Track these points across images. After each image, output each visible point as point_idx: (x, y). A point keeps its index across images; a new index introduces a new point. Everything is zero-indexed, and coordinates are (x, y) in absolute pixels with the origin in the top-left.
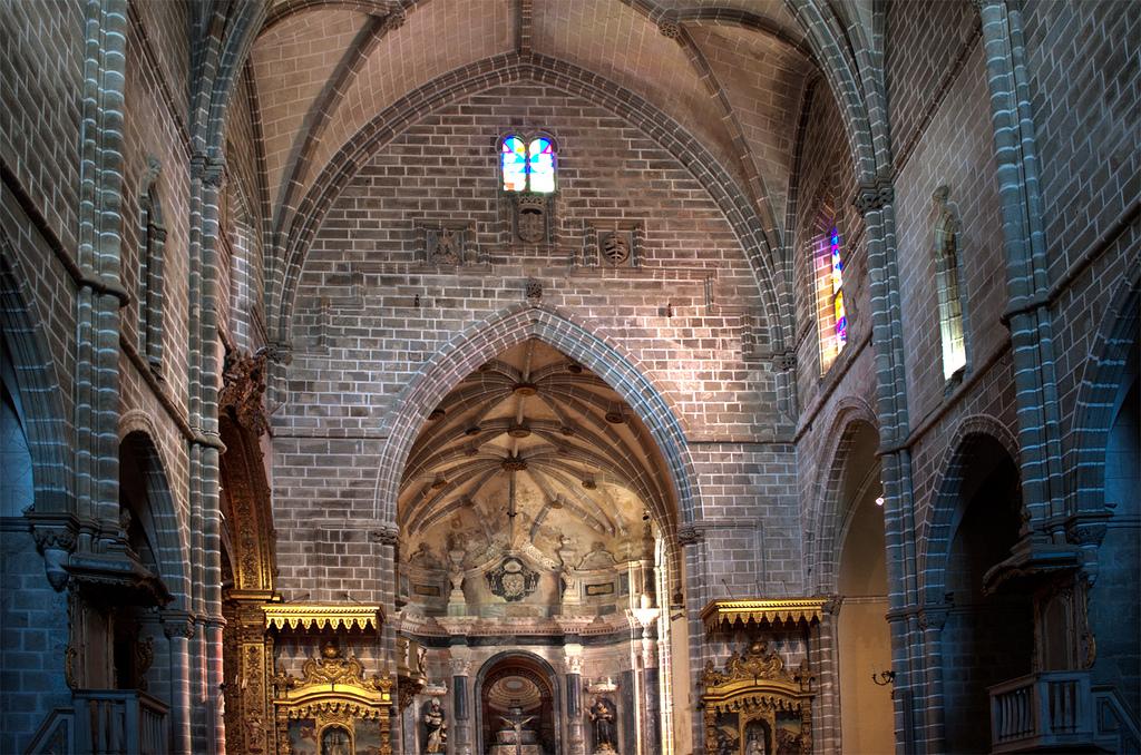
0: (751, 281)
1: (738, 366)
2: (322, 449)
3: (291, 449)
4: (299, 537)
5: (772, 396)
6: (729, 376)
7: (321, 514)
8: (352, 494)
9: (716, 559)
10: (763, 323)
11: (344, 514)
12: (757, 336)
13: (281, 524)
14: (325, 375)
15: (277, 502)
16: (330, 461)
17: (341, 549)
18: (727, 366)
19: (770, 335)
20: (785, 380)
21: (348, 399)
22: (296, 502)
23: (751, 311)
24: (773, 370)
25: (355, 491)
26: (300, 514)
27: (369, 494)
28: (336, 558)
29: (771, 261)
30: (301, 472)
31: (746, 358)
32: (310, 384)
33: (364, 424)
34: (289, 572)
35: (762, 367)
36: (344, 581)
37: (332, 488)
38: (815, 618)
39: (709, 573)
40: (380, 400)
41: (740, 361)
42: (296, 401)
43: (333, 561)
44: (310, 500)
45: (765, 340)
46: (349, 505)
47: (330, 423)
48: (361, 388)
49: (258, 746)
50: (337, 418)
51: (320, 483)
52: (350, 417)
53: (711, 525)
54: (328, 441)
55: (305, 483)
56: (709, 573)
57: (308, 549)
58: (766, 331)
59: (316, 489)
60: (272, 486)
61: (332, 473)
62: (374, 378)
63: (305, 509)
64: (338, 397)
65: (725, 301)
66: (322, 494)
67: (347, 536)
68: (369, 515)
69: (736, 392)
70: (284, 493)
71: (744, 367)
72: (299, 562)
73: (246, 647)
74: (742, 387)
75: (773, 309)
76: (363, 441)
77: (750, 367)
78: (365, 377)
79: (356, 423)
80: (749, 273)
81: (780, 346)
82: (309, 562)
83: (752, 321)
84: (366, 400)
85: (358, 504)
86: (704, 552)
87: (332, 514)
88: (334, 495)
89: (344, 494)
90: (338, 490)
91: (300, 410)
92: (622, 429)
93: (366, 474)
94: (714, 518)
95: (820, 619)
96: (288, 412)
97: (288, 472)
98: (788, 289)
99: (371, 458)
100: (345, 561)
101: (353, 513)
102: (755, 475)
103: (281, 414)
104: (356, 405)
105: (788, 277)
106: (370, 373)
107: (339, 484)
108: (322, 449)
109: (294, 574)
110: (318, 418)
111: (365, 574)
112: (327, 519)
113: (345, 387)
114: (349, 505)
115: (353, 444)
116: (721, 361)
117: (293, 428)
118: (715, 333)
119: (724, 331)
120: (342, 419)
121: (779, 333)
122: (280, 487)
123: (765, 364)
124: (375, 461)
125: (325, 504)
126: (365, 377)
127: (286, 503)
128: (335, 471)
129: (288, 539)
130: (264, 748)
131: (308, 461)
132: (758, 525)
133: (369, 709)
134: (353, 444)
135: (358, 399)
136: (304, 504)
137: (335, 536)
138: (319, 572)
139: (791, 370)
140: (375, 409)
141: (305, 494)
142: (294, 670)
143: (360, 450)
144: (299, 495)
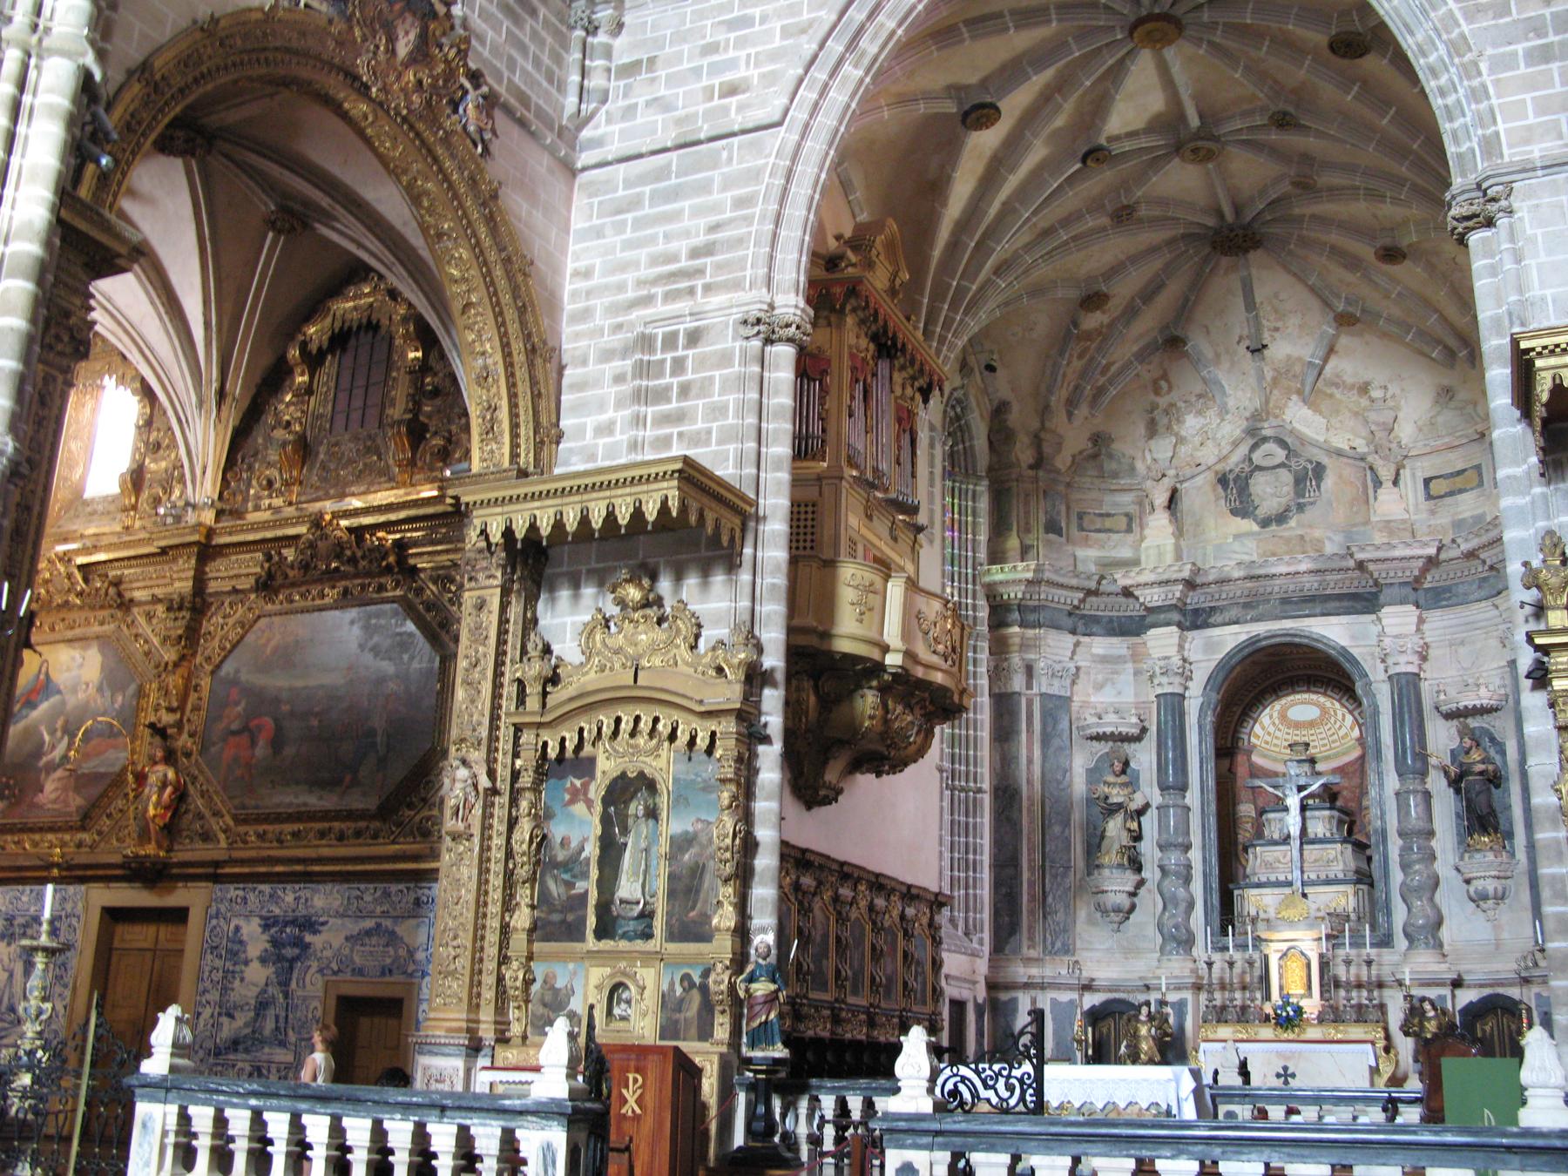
2: (662, 174)
3: (609, 186)
4: (607, 355)
7: (648, 300)
8: (708, 250)
9: (1550, 252)
11: (691, 291)
13: (577, 336)
14: (680, 37)
15: (575, 295)
16: (675, 194)
17: (679, 366)
21: (715, 69)
22: (606, 287)
25: (714, 243)
26: (614, 309)
27: (740, 242)
28: (668, 388)
30: (620, 228)
32: (652, 61)
33: (740, 108)
34: (581, 430)
36: (680, 435)
37: (674, 246)
39: (1535, 292)
40: (774, 56)
42: (625, 96)
43: (661, 395)
44: (630, 277)
46: (700, 272)
47: (679, 122)
48: (741, 43)
49: (461, 826)
50: (692, 110)
51: (652, 240)
52: (716, 102)
53: (1527, 169)
54: (674, 155)
55: (629, 245)
56: (1535, 292)
57: (619, 379)
59: (643, 254)
60: (570, 266)
61: (675, 216)
62: (764, 19)
63: (621, 297)
64: (697, 72)
66: (654, 261)
67: (694, 338)
68: (737, 285)
70: (587, 274)
72: (602, 407)
73: (469, 598)
76: (735, 140)
78: (746, 22)
79: (725, 110)
82: (619, 404)
84: (748, 63)
85: (719, 267)
86: (1512, 238)
87: (670, 297)
88: (674, 258)
89: (695, 253)
90: (682, 246)
91: (630, 111)
92: (1373, 64)
93: (740, 203)
94: (1537, 151)
96: (609, 121)
97: (599, 233)
99: (749, 170)
100: (685, 390)
101: (708, 288)
103: (596, 127)
104: (729, 76)
106: (756, 12)
107: (687, 234)
108: (662, 174)
109: (589, 433)
110: (660, 118)
111: (718, 411)
112: (660, 309)
113: (712, 48)
114: (700, 272)
115: (718, 152)
117: (612, 150)
120: (701, 108)
122: (582, 264)
124: (755, 175)
125: (656, 281)
126: (746, 22)
127: (589, 293)
128: (680, 212)
129: (584, 362)
130: (476, 830)
131: (635, 203)
133: (696, 723)
134: (718, 152)
135: (732, 64)
136: (621, 287)
137: (670, 341)
138: (639, 421)
140: (763, 76)
141: (623, 267)
142: (567, 649)
143: (730, 159)
144: (613, 272)
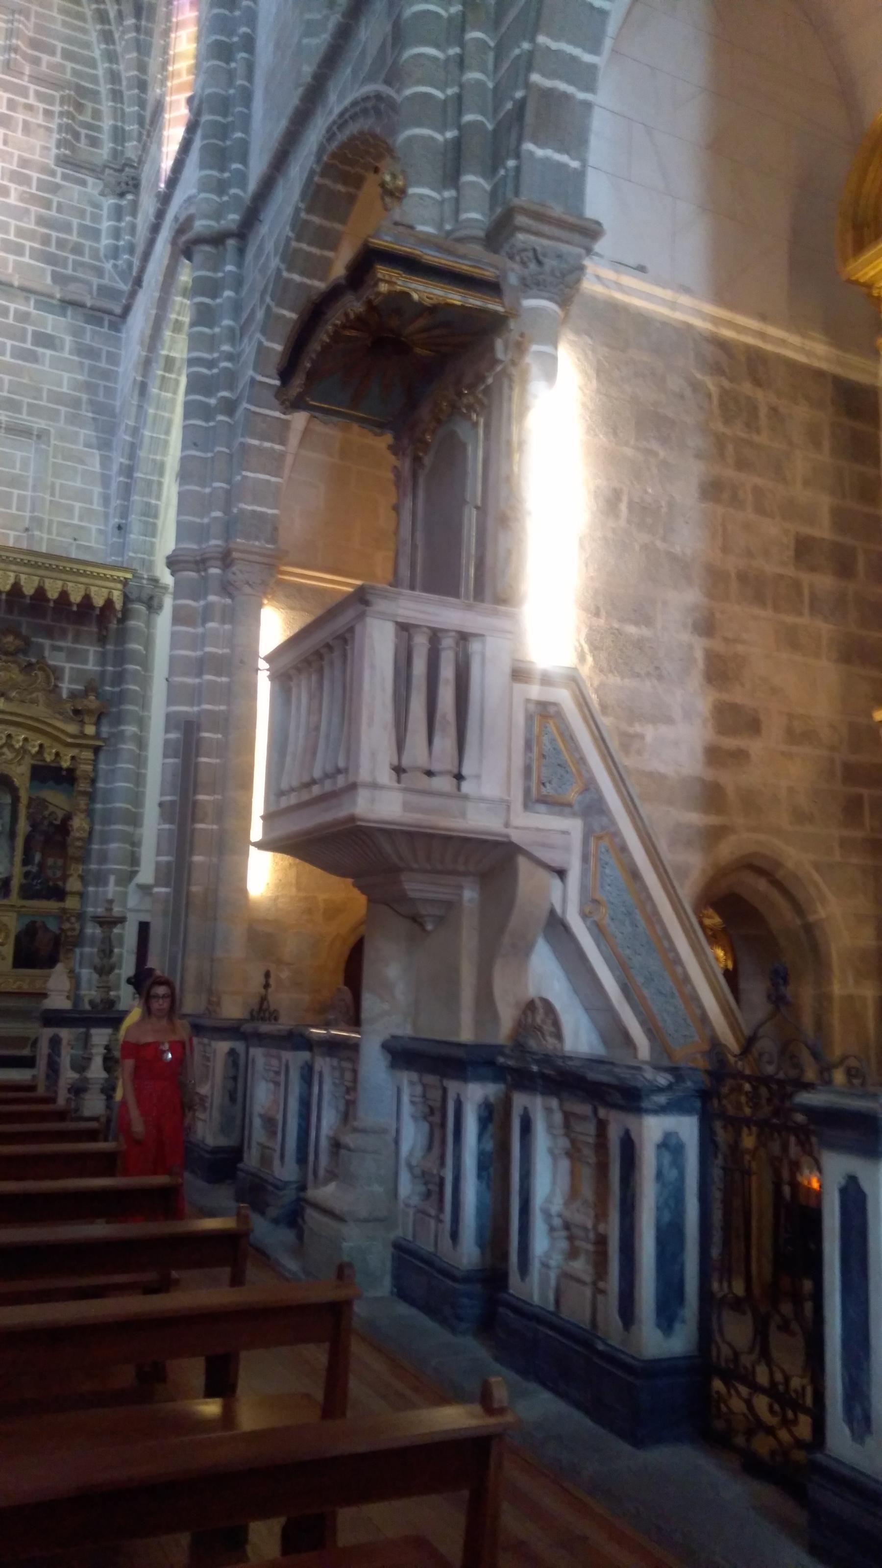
0: (87, 45)
1: (45, 169)
5: (94, 234)
6: (23, 180)
10: (97, 115)
12: (83, 132)
18: (24, 163)
19: (105, 137)
20: (118, 213)
23: (79, 89)
24: (102, 194)
29: (120, 15)
31: (62, 161)
35: (83, 183)
38: (109, 603)
41: (51, 163)
45: (94, 142)
58: (98, 129)
65: (36, 61)
69: (35, 210)
71: (53, 174)
74: (47, 204)
75: (117, 95)
77: (65, 177)
80: (84, 31)
81: (115, 154)
83: (80, 107)
95: (118, 605)
98: (142, 67)
102: (49, 352)
105: (142, 48)
116: (16, 153)
118: (12, 105)
119: (29, 108)
121: (119, 136)
123: (90, 180)
132: (42, 435)
139: (130, 197)
